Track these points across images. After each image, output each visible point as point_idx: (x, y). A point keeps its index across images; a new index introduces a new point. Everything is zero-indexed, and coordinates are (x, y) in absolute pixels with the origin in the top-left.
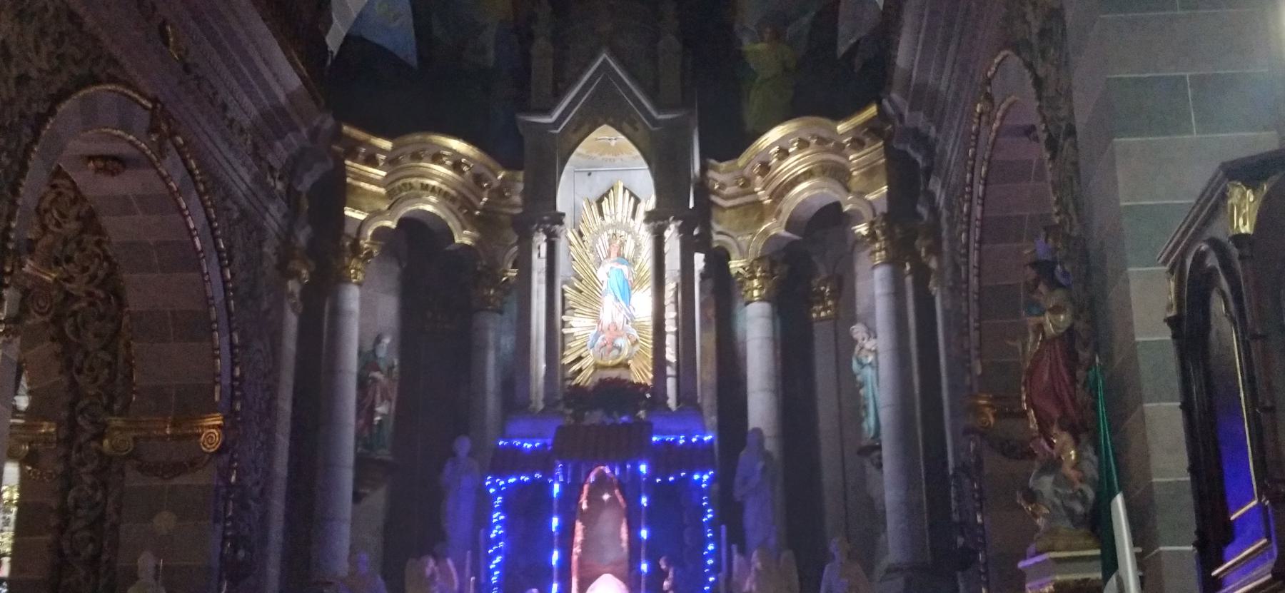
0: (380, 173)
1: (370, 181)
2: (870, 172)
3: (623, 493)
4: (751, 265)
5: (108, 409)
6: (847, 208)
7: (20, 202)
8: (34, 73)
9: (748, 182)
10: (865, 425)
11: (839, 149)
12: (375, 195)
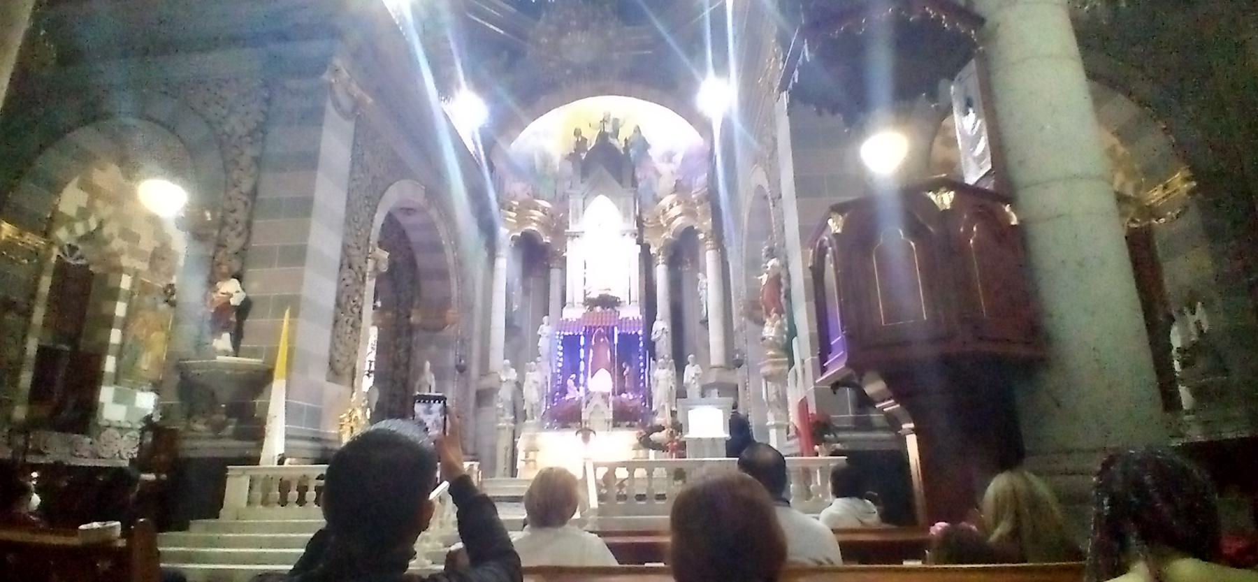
0: (514, 215)
1: (510, 217)
2: (705, 213)
3: (608, 339)
4: (659, 250)
5: (412, 306)
6: (696, 228)
7: (374, 225)
8: (378, 175)
9: (658, 217)
10: (702, 312)
11: (693, 204)
12: (512, 223)
